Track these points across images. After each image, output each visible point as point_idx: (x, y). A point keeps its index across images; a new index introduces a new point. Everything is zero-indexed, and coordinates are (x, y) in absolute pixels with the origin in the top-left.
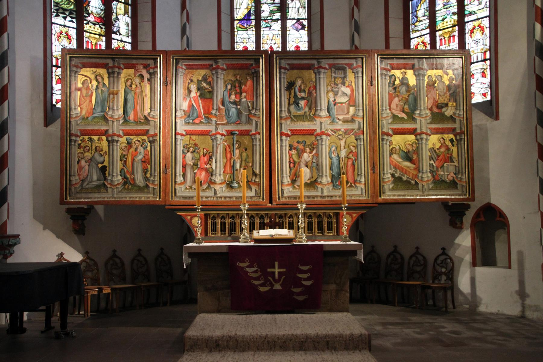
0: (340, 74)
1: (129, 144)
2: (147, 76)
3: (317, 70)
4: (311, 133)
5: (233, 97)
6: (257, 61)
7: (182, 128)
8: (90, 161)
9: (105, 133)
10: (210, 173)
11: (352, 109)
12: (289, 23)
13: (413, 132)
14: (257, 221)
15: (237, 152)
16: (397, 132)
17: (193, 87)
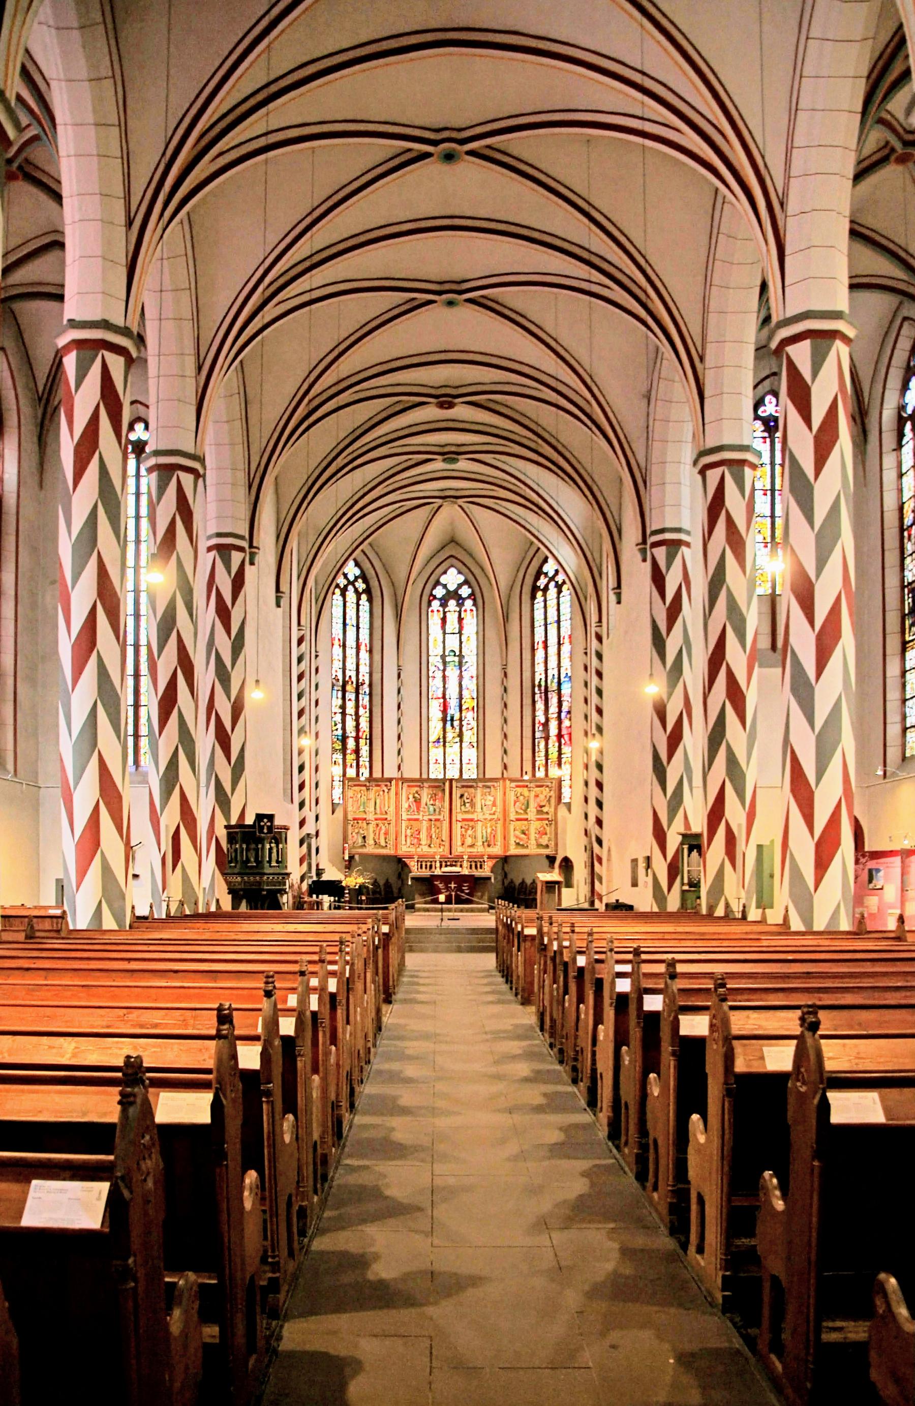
0: (488, 790)
1: (377, 825)
2: (386, 791)
3: (476, 788)
4: (472, 820)
5: (432, 802)
6: (444, 784)
7: (405, 817)
8: (357, 833)
9: (365, 819)
10: (419, 839)
11: (494, 808)
12: (464, 745)
13: (526, 820)
14: (444, 864)
15: (433, 830)
16: (518, 820)
17: (411, 796)
